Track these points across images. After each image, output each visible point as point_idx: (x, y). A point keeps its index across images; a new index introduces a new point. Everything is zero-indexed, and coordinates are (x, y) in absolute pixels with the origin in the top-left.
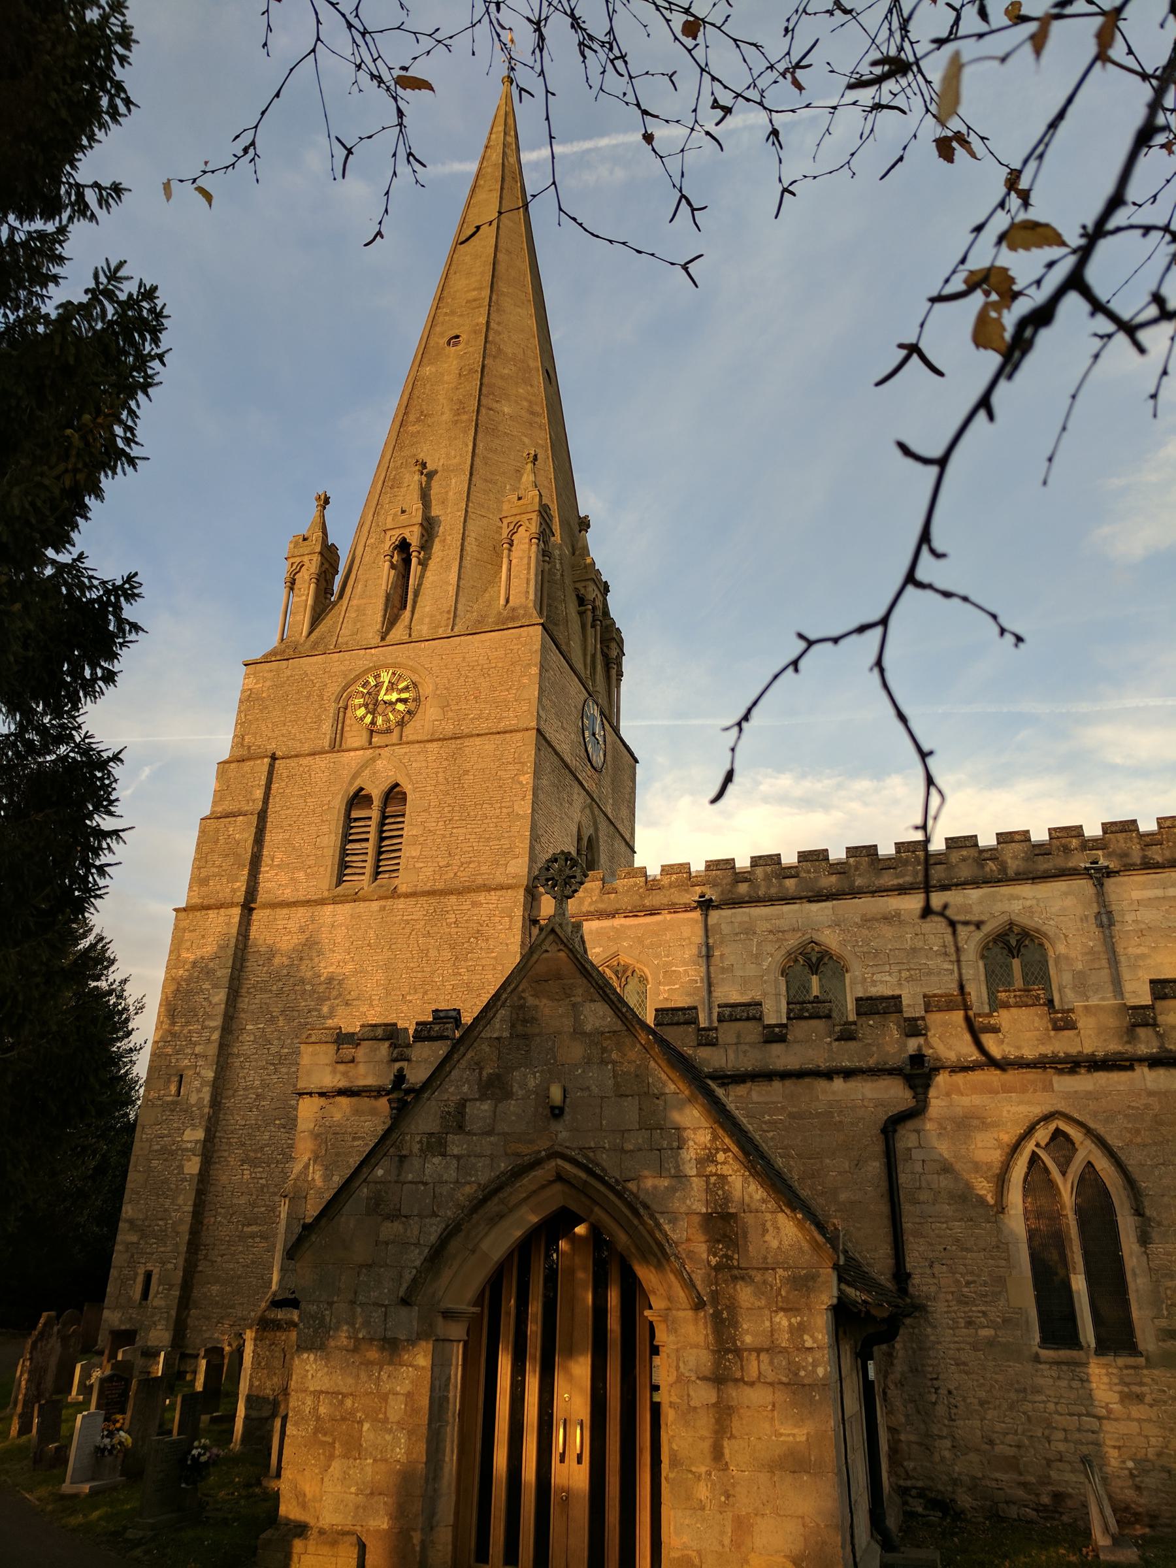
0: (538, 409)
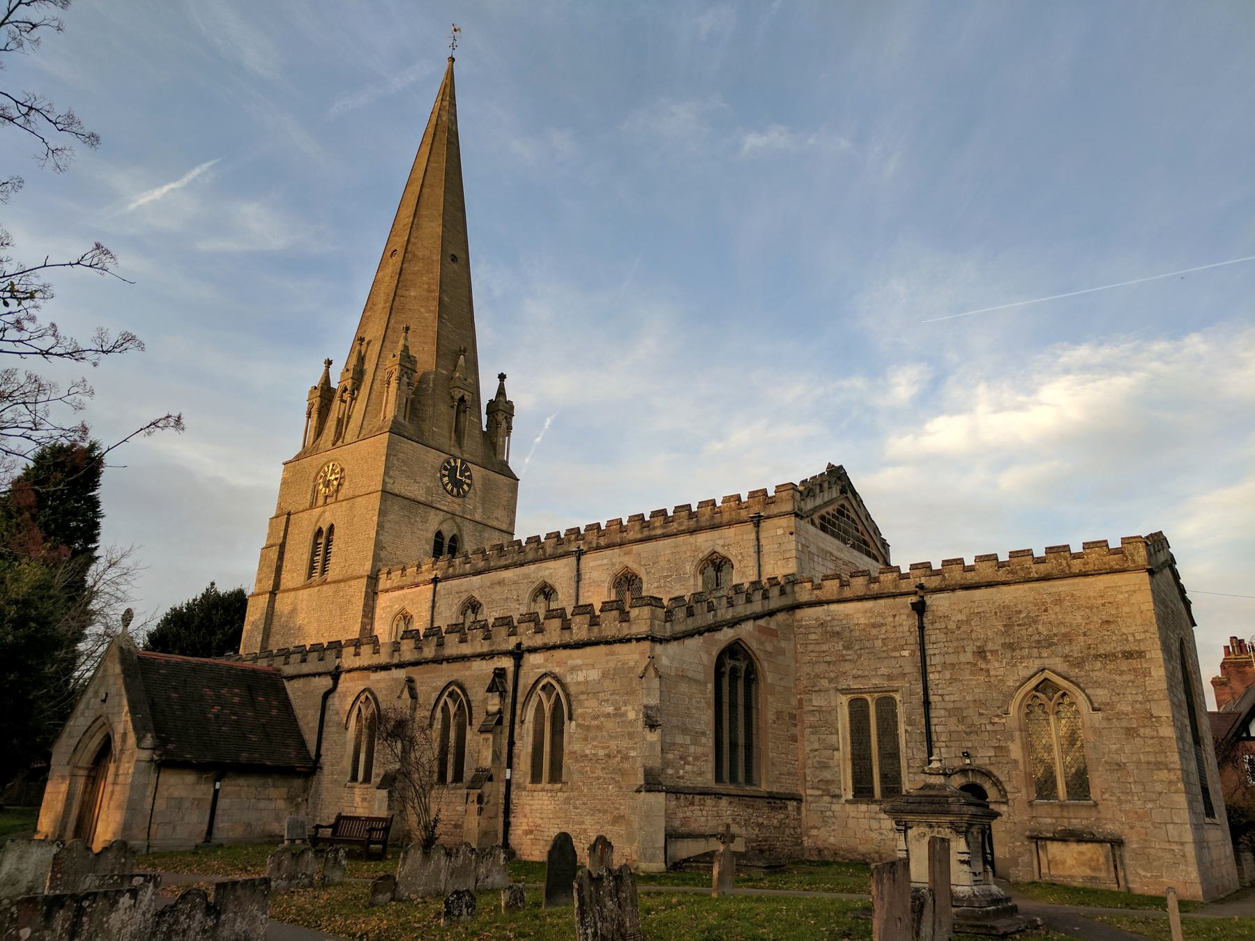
0: (434, 287)
